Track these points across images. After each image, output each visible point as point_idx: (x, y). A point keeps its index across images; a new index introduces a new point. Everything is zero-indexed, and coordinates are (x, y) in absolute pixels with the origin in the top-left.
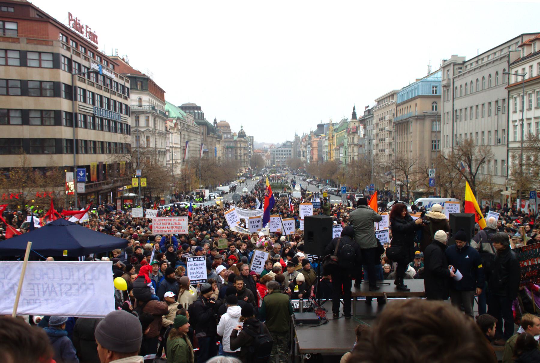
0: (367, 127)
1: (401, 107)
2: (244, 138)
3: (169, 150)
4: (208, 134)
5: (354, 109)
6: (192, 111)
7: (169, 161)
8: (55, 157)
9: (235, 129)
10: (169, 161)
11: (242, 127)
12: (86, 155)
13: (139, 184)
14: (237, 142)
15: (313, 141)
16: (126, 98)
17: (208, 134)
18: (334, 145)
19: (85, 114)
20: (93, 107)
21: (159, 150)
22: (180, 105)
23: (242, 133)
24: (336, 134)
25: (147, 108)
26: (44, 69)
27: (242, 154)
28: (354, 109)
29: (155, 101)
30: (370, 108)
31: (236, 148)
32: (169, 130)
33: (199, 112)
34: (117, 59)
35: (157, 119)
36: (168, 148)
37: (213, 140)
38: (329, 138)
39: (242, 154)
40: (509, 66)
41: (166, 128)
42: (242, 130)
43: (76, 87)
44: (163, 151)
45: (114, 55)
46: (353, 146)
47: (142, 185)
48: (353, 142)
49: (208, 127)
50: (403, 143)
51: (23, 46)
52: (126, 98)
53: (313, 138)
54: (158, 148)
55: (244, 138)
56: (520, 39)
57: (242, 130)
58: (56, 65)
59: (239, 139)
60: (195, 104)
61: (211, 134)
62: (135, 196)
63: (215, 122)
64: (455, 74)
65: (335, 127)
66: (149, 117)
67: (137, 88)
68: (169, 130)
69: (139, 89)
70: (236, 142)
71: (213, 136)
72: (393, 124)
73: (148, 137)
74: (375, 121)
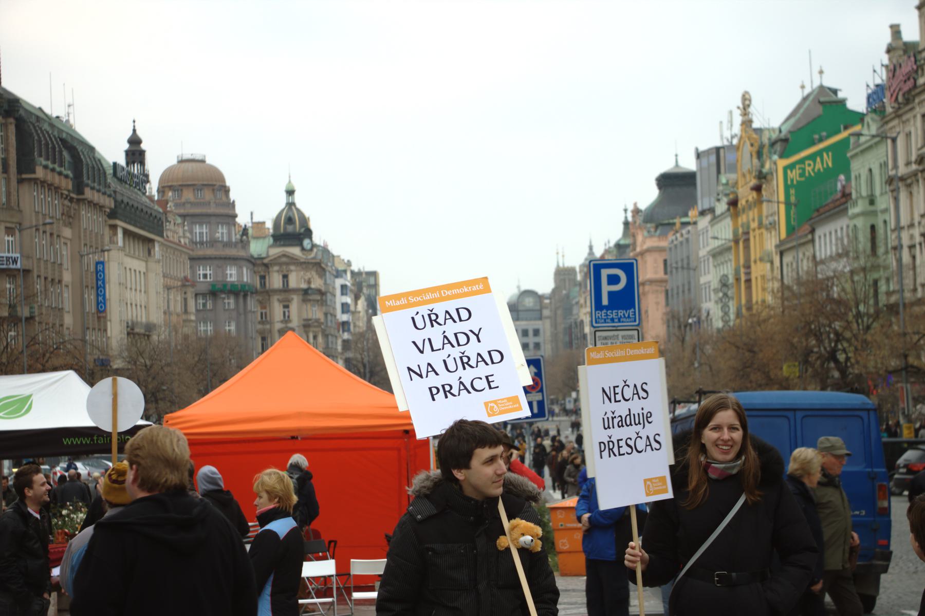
4: (25, 164)
11: (290, 192)
14: (266, 266)
17: (25, 164)
18: (773, 226)
23: (290, 220)
24: (782, 163)
42: (291, 205)
49: (17, 127)
53: (640, 238)
57: (291, 205)
59: (276, 251)
70: (261, 265)
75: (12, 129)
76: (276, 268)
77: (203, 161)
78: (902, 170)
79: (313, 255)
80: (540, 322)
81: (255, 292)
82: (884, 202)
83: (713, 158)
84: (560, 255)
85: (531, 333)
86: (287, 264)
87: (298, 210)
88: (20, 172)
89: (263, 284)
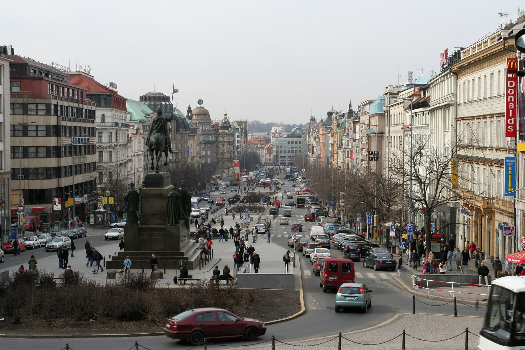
0: (357, 131)
2: (228, 130)
3: (131, 159)
4: (178, 130)
5: (350, 106)
6: (158, 103)
7: (130, 171)
8: (46, 181)
9: (216, 117)
10: (130, 171)
11: (226, 115)
12: (66, 178)
13: (108, 200)
14: (218, 134)
16: (93, 122)
19: (65, 145)
20: (70, 139)
21: (121, 162)
22: (143, 94)
25: (110, 125)
26: (40, 116)
27: (225, 151)
28: (350, 106)
29: (117, 114)
31: (218, 142)
32: (131, 138)
33: (167, 103)
36: (129, 158)
37: (184, 137)
39: (225, 151)
40: (404, 110)
41: (128, 136)
43: (60, 126)
45: (78, 70)
47: (110, 203)
48: (348, 145)
49: (176, 122)
51: (26, 100)
52: (93, 122)
54: (120, 161)
56: (413, 89)
57: (226, 118)
58: (48, 113)
60: (162, 94)
61: (182, 130)
62: (105, 212)
64: (391, 103)
66: (111, 133)
67: (101, 104)
68: (131, 138)
69: (102, 105)
71: (184, 132)
73: (111, 152)
75: (176, 122)
76: (221, 136)
77: (203, 108)
79: (231, 132)
80: (302, 139)
81: (216, 142)
84: (313, 111)
85: (298, 142)
86: (224, 135)
87: (227, 120)
88: (177, 131)
89: (217, 140)
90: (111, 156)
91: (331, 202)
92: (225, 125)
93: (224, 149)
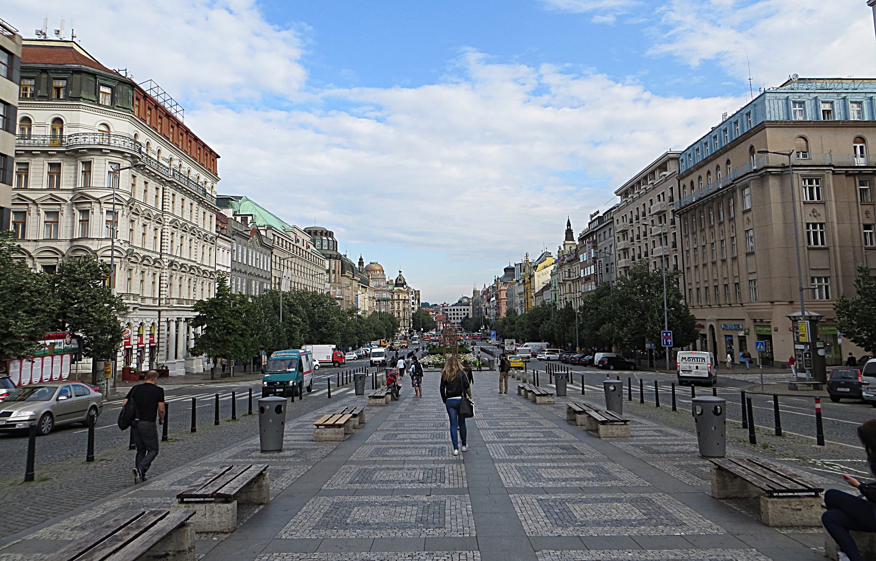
0: (599, 245)
1: (694, 177)
2: (403, 286)
4: (343, 272)
5: (569, 224)
15: (500, 291)
17: (343, 272)
28: (569, 224)
29: (166, 153)
30: (601, 214)
33: (330, 239)
34: (72, 48)
35: (170, 191)
38: (524, 281)
44: (191, 268)
46: (571, 282)
48: (569, 277)
50: (708, 246)
55: (403, 286)
63: (361, 263)
65: (533, 265)
67: (98, 101)
70: (392, 292)
72: (670, 216)
74: (619, 226)
75: (340, 263)
78: (561, 281)
82: (558, 288)
83: (519, 267)
90: (113, 224)
91: (664, 337)
92: (400, 282)
93: (399, 308)
